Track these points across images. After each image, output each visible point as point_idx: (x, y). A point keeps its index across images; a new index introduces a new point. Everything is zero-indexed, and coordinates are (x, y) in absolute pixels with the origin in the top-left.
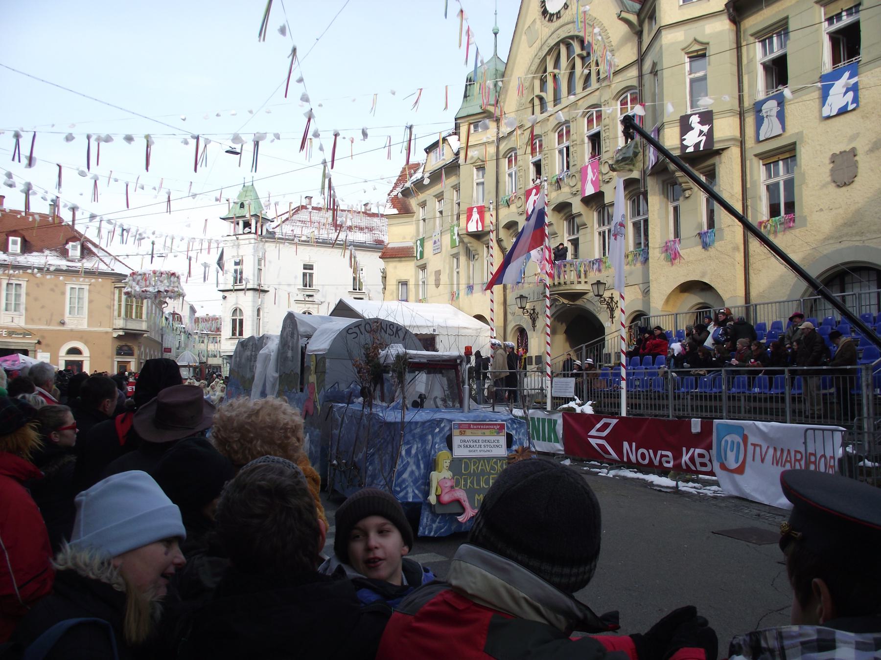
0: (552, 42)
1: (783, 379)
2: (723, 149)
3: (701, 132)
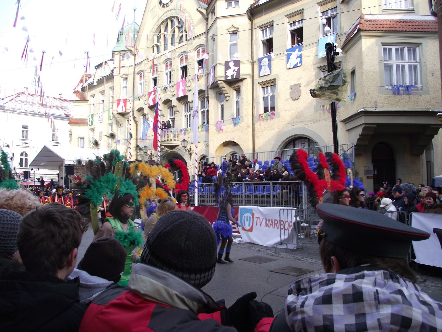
0: (164, 18)
1: (269, 187)
2: (244, 79)
3: (234, 70)
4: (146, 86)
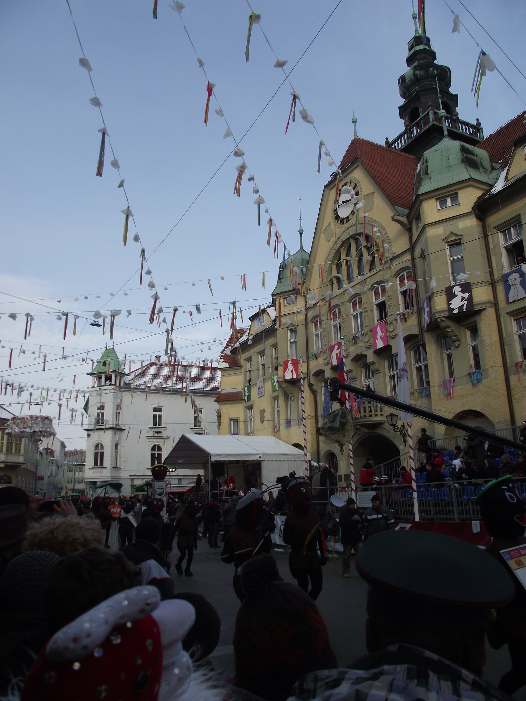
0: (344, 238)
2: (482, 310)
3: (463, 298)
4: (325, 338)
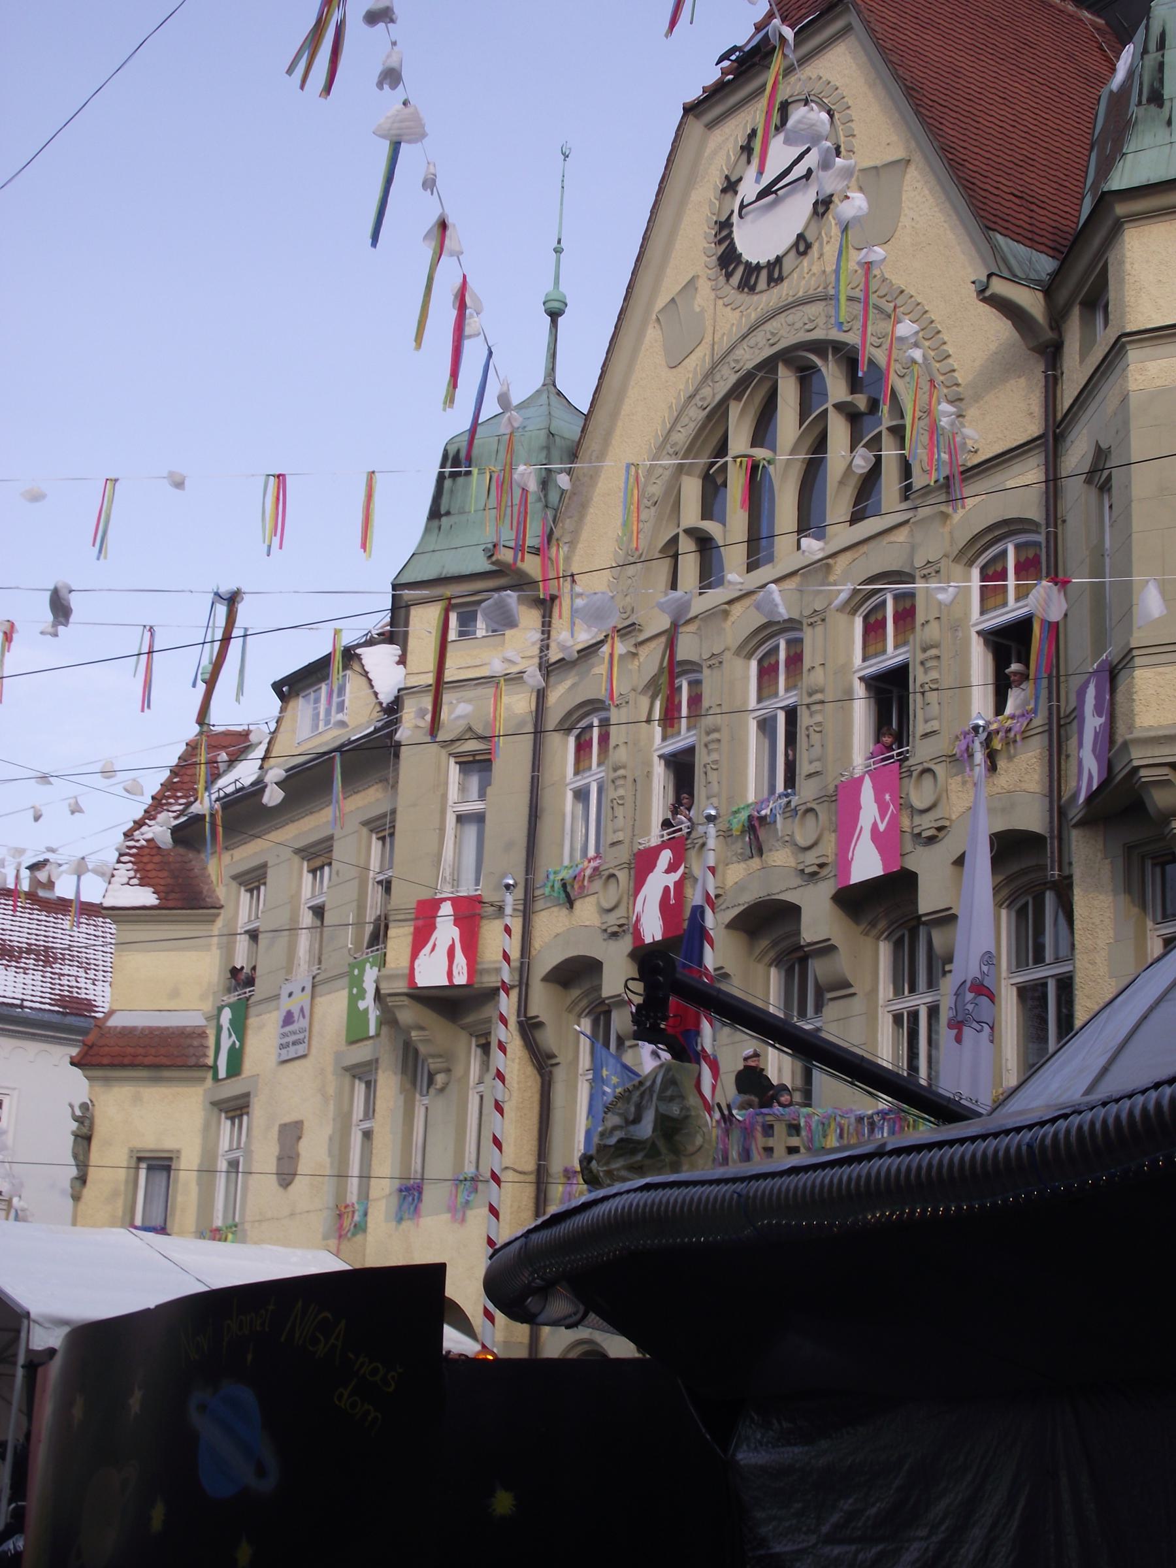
0: (750, 356)
4: (620, 811)
